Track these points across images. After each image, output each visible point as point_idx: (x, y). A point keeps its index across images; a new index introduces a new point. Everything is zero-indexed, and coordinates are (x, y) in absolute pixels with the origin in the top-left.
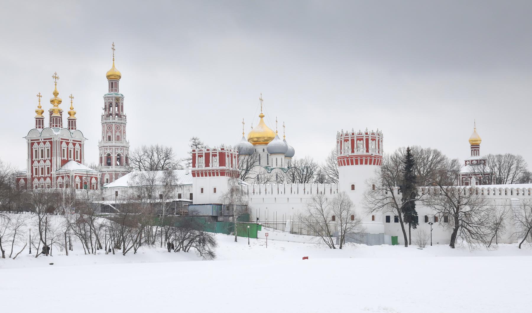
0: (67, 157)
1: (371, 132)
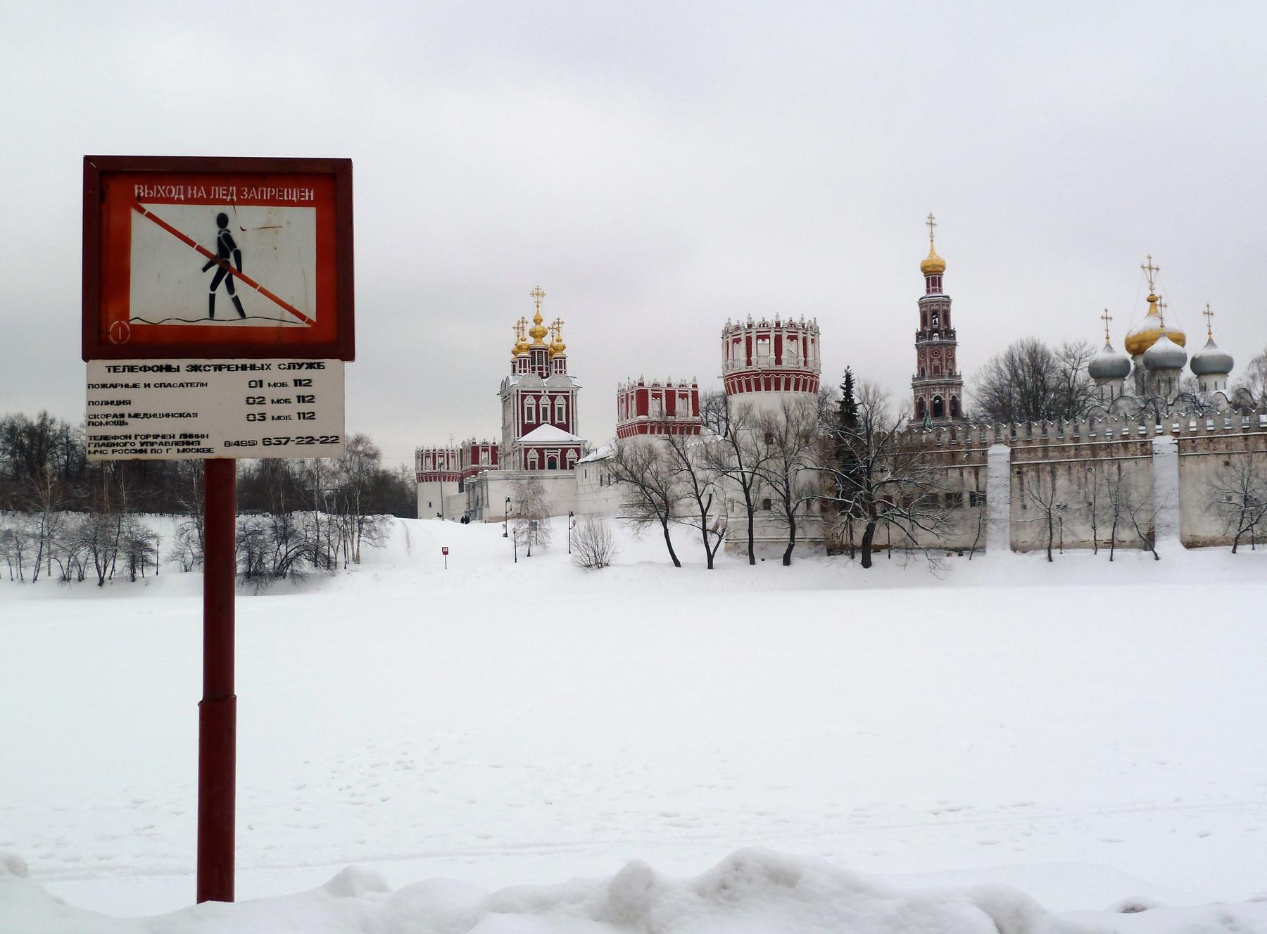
0: (538, 419)
1: (787, 321)
